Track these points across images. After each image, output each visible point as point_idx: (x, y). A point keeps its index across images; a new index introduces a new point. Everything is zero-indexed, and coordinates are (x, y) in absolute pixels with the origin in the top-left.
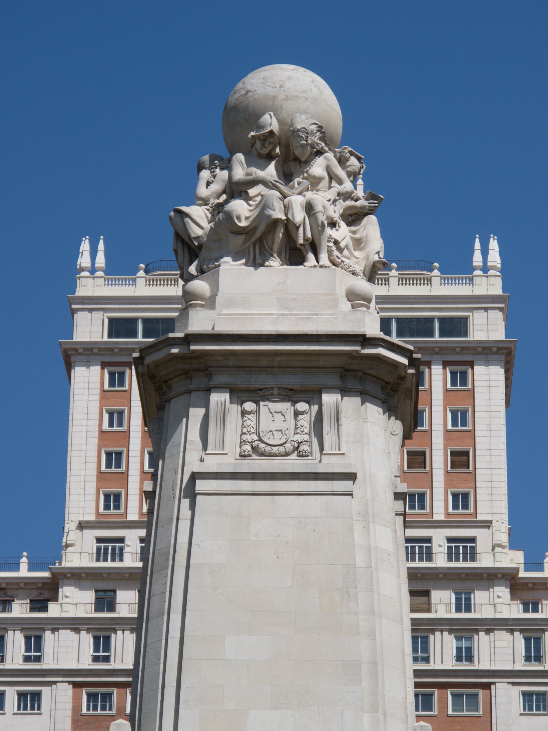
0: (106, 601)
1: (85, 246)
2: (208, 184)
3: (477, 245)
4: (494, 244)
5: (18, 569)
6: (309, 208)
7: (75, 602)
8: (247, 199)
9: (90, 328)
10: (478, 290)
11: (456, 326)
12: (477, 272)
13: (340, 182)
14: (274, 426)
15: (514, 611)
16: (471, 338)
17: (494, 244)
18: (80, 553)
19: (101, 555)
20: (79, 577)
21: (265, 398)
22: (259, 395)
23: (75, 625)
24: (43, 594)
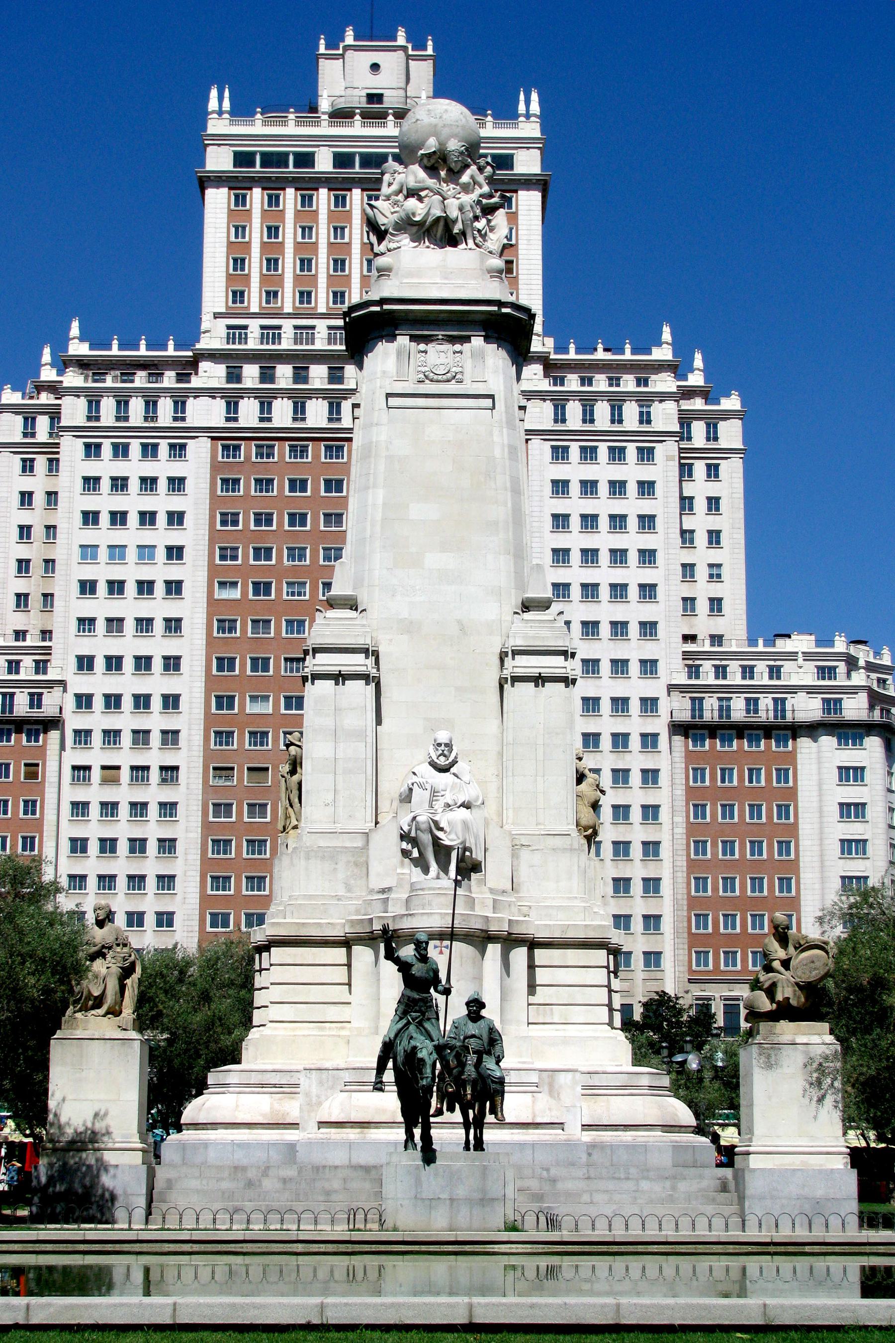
0: (234, 375)
1: (214, 93)
2: (390, 185)
3: (522, 97)
4: (534, 96)
5: (166, 350)
6: (461, 209)
7: (211, 374)
8: (420, 199)
9: (219, 160)
10: (522, 134)
11: (504, 162)
12: (522, 119)
13: (481, 187)
14: (438, 362)
15: (545, 385)
16: (515, 172)
17: (534, 96)
18: (213, 337)
19: (230, 339)
20: (214, 356)
21: (432, 341)
22: (427, 339)
23: (212, 393)
24: (187, 368)
